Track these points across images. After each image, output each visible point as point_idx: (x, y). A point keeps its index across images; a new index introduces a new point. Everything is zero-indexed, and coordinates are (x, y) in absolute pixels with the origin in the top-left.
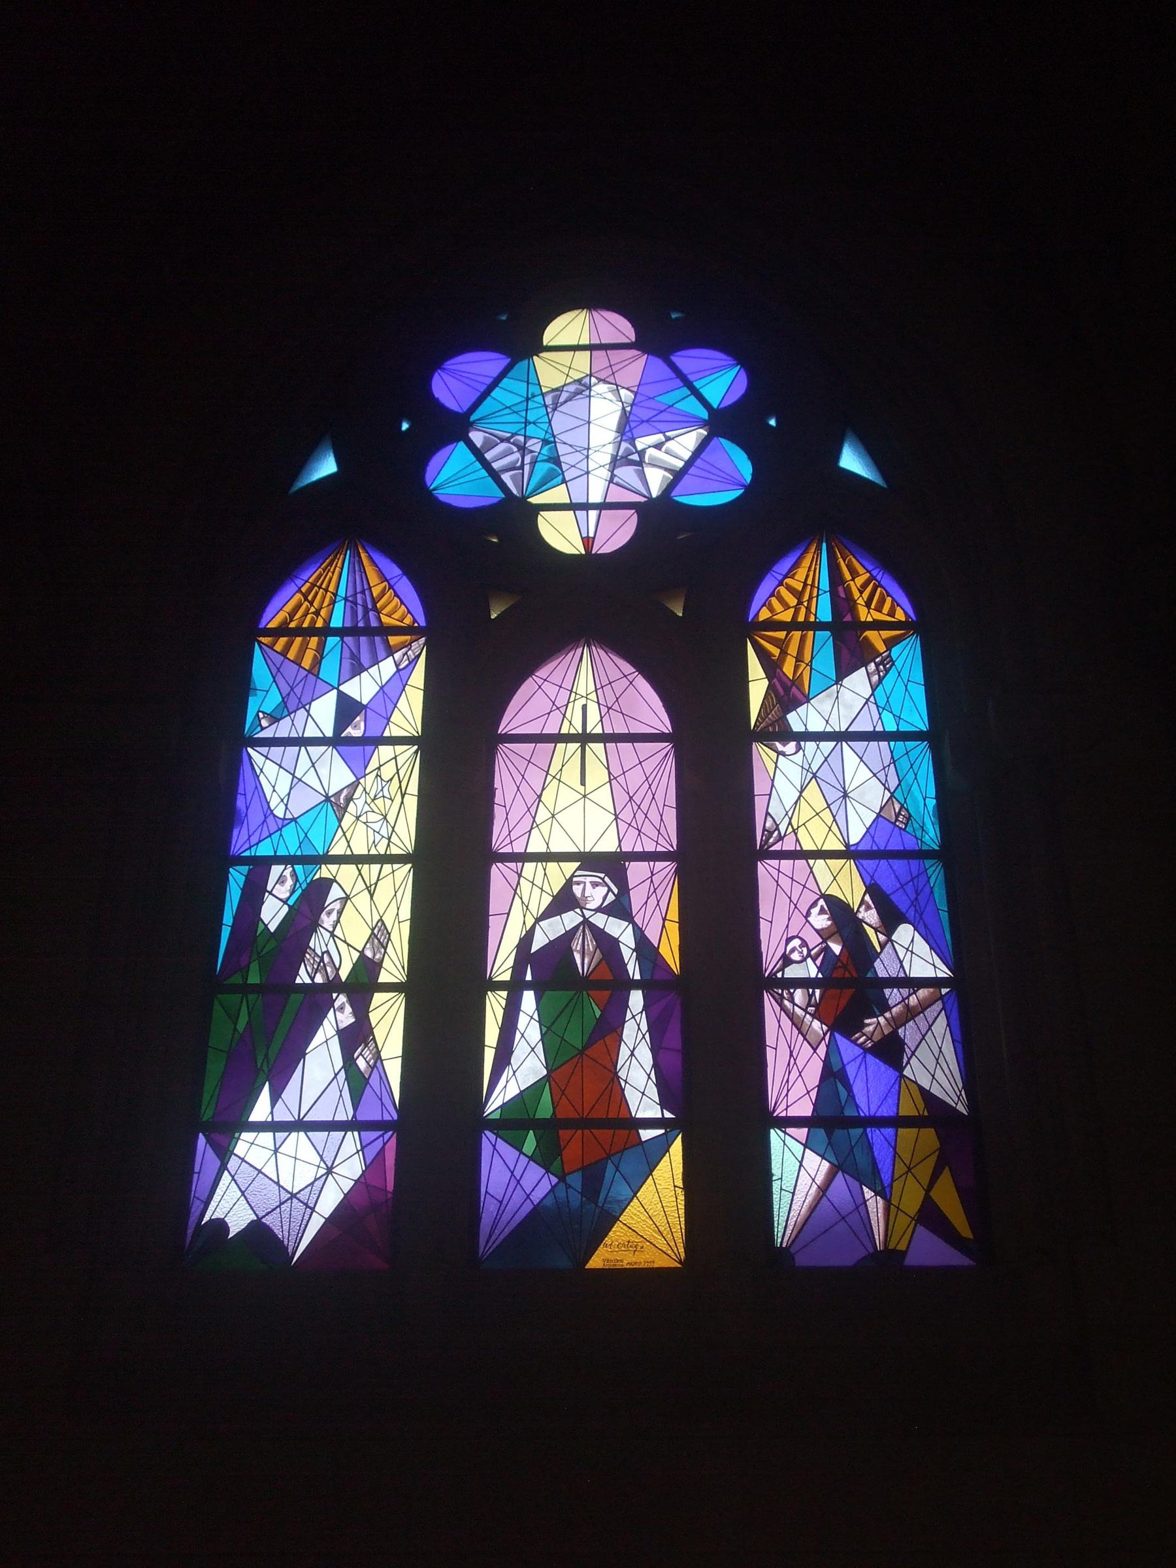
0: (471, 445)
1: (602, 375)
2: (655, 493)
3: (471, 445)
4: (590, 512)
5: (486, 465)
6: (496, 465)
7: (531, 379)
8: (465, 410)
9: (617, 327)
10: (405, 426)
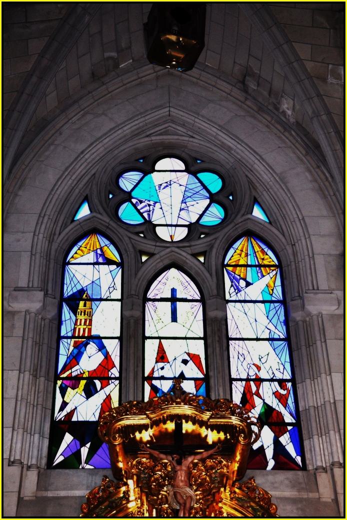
4: (173, 227)
5: (138, 211)
6: (141, 211)
7: (151, 181)
8: (129, 191)
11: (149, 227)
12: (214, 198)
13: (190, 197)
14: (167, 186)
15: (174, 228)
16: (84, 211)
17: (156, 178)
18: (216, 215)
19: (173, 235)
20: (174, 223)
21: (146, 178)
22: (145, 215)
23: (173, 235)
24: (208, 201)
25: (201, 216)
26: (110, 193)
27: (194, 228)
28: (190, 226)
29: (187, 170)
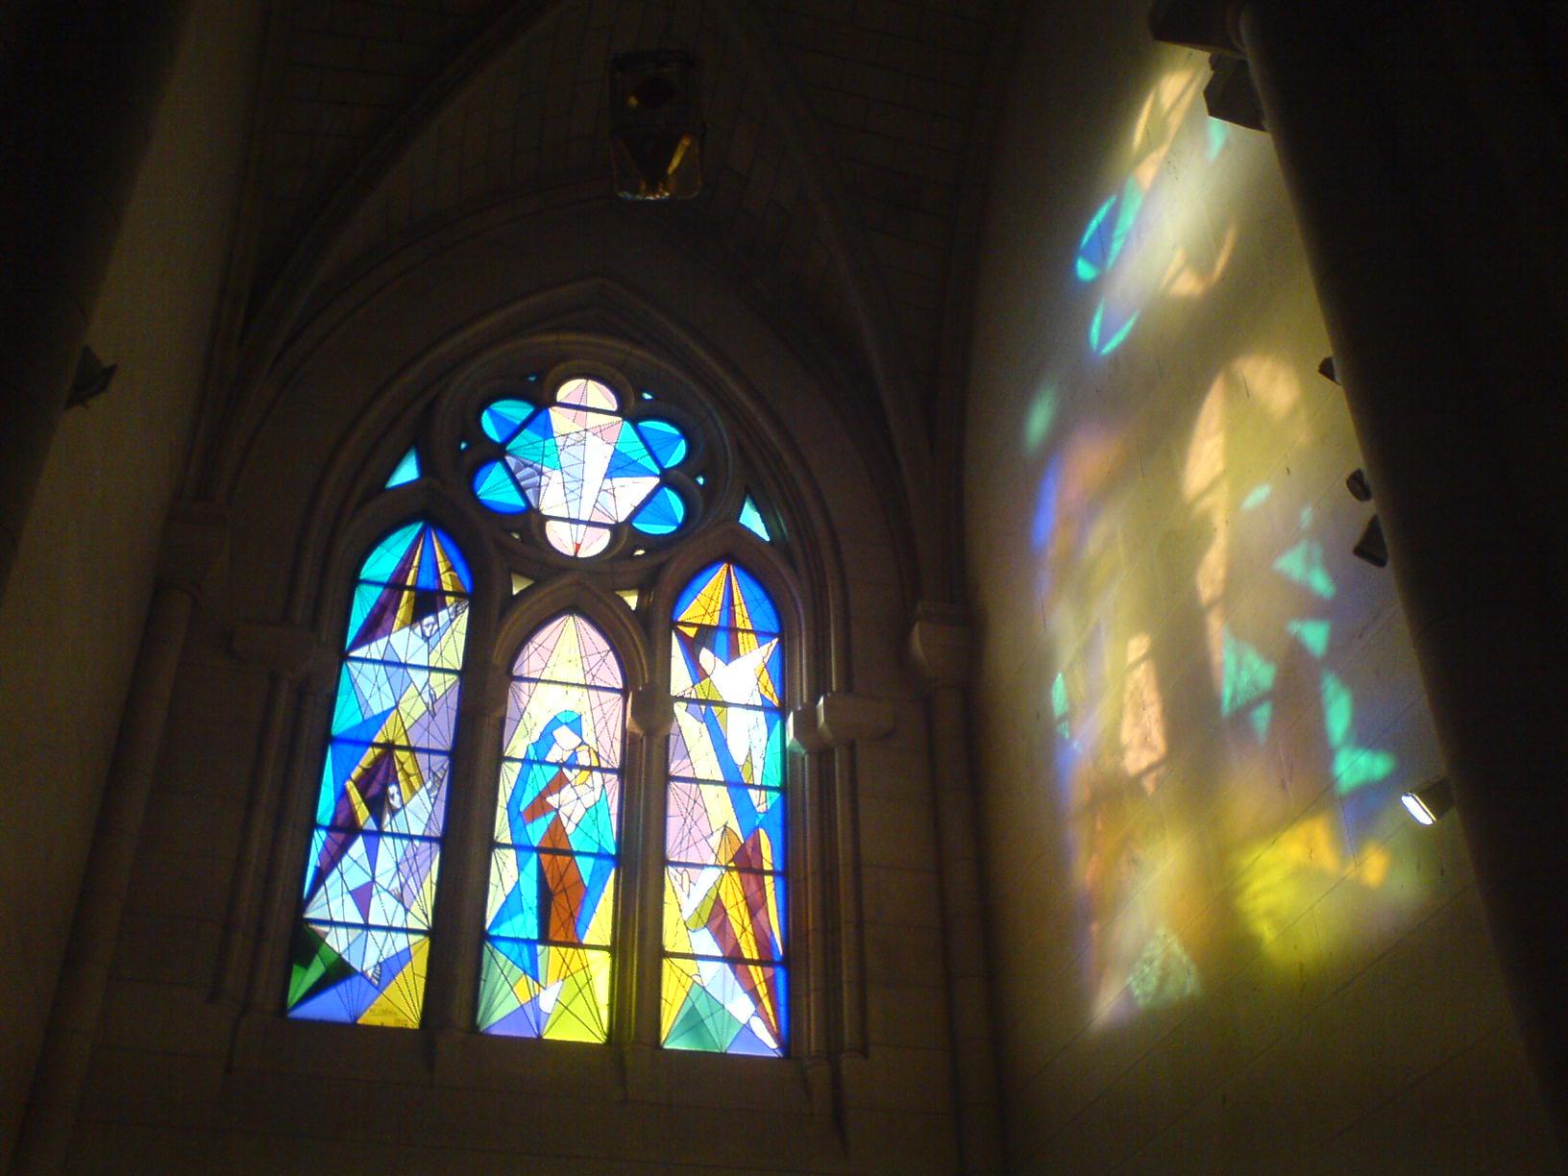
2: (621, 519)
11: (531, 521)
15: (582, 527)
16: (407, 472)
20: (584, 517)
21: (541, 418)
22: (529, 493)
24: (656, 481)
26: (462, 439)
27: (621, 532)
28: (616, 529)
29: (620, 412)
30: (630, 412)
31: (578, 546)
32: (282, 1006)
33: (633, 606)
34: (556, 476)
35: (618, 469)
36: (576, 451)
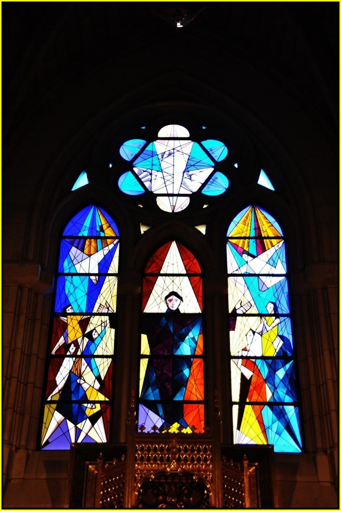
0: (134, 173)
1: (178, 149)
3: (134, 173)
9: (183, 132)
10: (111, 166)
11: (149, 197)
12: (219, 167)
13: (193, 165)
14: (170, 154)
15: (175, 198)
16: (82, 181)
17: (158, 146)
18: (221, 185)
19: (174, 205)
20: (176, 192)
21: (151, 144)
23: (174, 205)
25: (204, 185)
27: (197, 198)
29: (192, 138)
30: (196, 137)
31: (174, 207)
32: (39, 446)
33: (204, 233)
34: (160, 174)
35: (192, 166)
36: (171, 158)
